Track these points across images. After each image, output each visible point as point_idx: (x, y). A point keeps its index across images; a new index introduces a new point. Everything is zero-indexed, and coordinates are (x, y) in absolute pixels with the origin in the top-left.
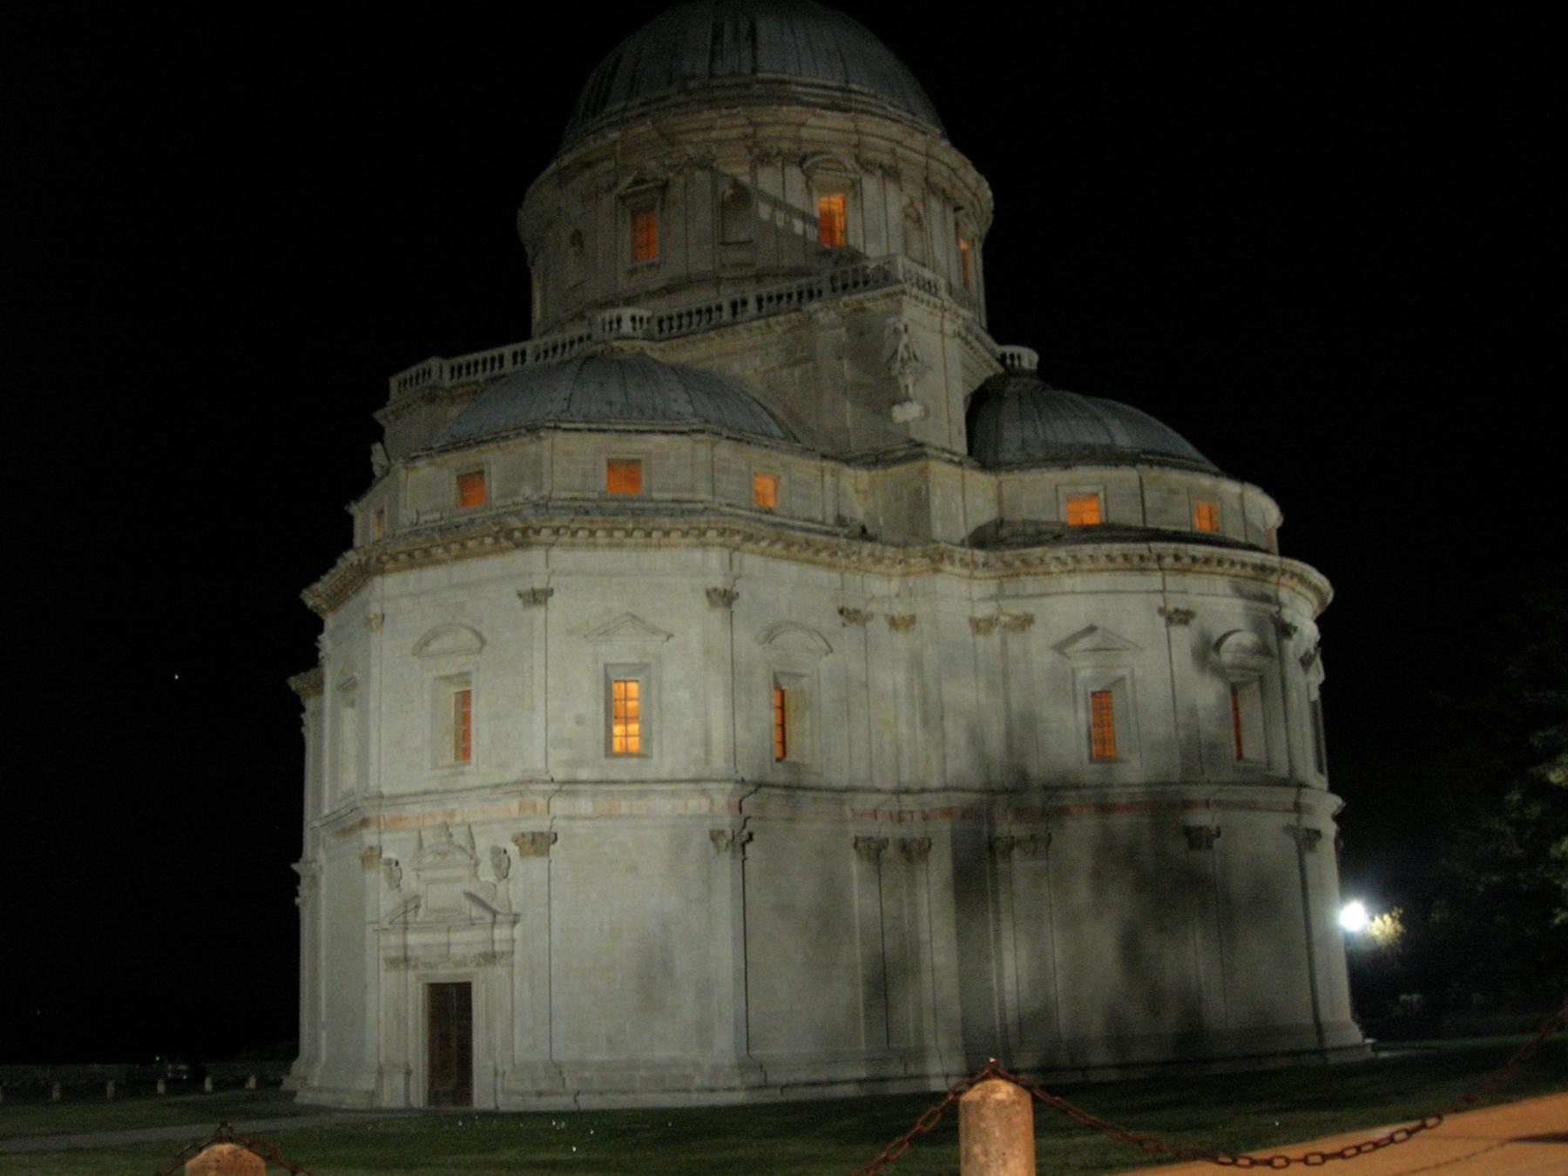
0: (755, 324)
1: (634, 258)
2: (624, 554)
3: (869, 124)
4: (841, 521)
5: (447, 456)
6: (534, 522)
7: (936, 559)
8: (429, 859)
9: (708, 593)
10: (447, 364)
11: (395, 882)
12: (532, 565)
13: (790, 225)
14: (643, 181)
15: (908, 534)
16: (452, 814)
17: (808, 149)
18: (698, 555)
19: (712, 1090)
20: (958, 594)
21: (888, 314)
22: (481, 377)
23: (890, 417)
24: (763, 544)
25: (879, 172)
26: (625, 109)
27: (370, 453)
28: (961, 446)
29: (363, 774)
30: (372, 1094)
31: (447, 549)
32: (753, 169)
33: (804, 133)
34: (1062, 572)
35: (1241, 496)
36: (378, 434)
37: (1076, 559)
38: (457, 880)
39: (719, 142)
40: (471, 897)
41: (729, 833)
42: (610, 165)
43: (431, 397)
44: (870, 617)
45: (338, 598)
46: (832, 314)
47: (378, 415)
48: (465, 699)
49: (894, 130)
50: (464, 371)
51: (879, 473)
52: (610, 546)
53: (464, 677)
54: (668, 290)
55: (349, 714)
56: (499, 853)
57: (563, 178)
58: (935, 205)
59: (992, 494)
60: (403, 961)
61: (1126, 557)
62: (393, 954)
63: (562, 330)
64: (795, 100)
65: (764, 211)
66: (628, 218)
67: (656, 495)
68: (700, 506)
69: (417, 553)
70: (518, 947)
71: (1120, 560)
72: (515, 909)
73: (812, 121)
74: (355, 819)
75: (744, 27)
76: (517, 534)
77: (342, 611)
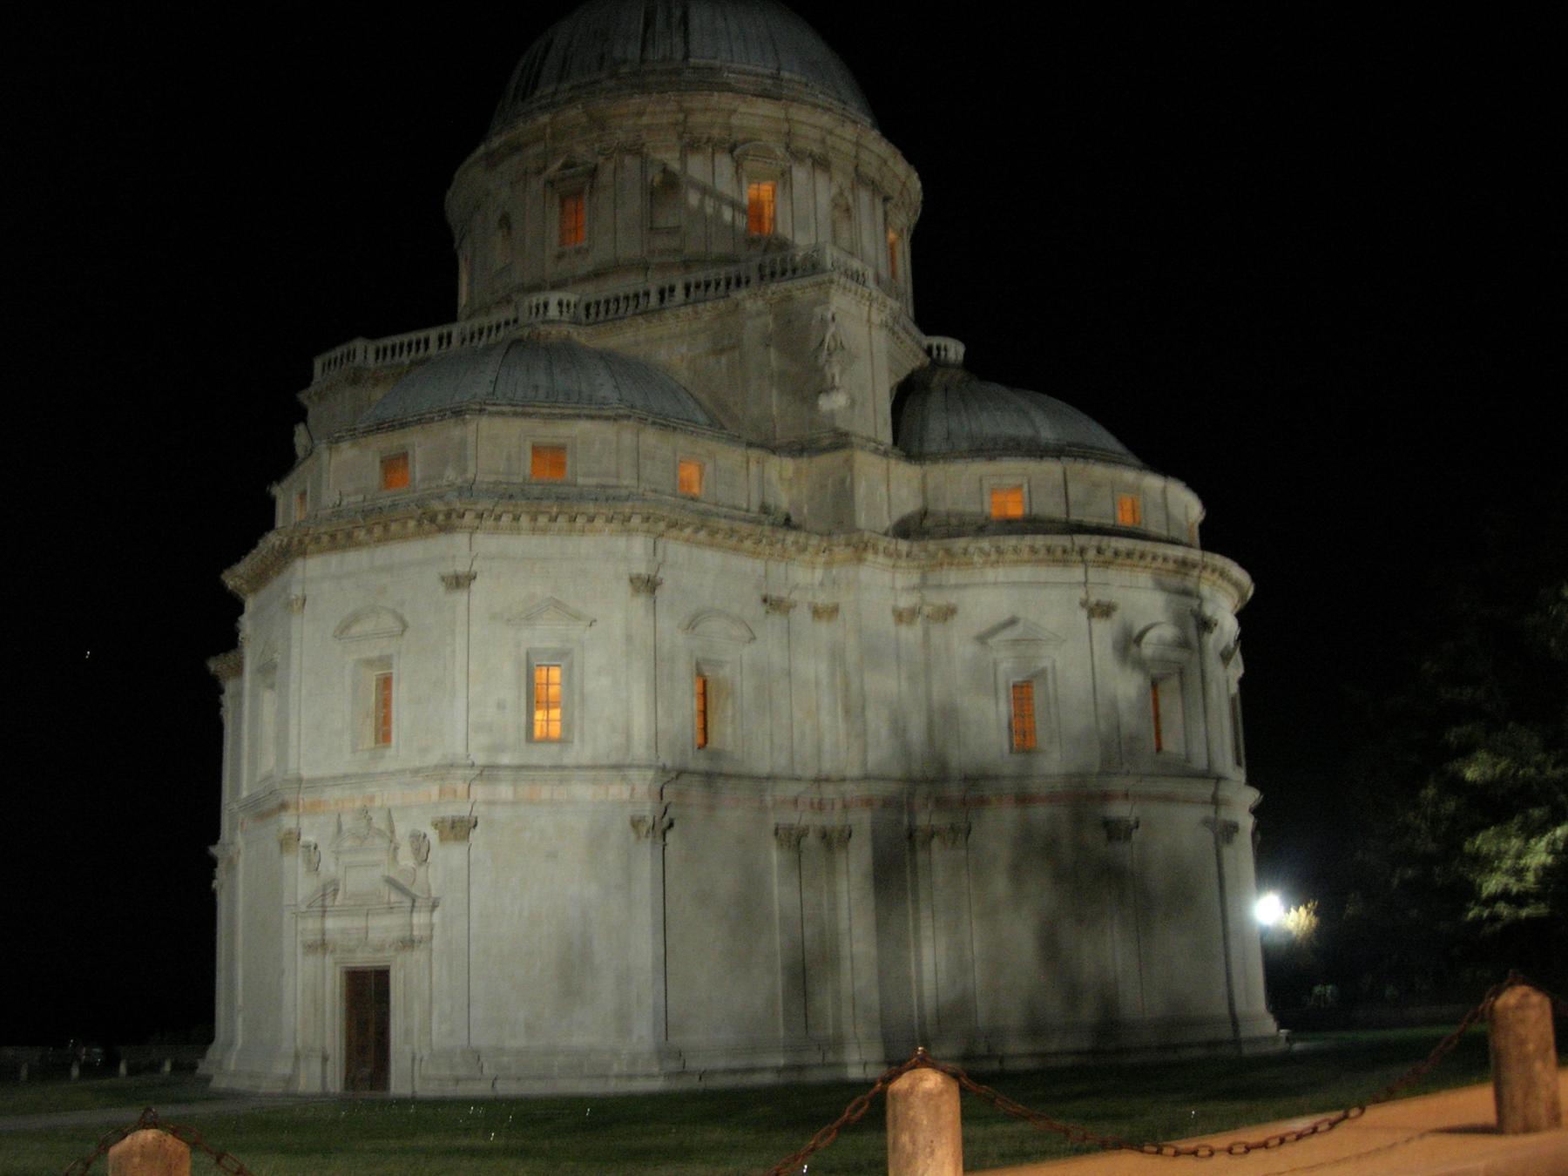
0: (683, 310)
1: (562, 243)
2: (548, 539)
3: (800, 114)
4: (765, 509)
5: (370, 438)
6: (458, 505)
7: (860, 549)
8: (348, 844)
9: (631, 581)
11: (313, 867)
12: (455, 550)
13: (718, 215)
14: (573, 165)
15: (835, 523)
16: (372, 799)
18: (621, 543)
19: (631, 1077)
20: (881, 585)
21: (815, 303)
22: (405, 359)
23: (814, 406)
24: (688, 531)
25: (809, 162)
26: (555, 93)
27: (292, 434)
28: (886, 436)
29: (282, 756)
30: (290, 1080)
31: (370, 531)
32: (683, 160)
33: (735, 121)
34: (986, 562)
35: (1164, 492)
36: (301, 415)
37: (999, 552)
38: (375, 865)
39: (648, 127)
40: (391, 882)
41: (650, 822)
42: (538, 149)
43: (356, 379)
44: (793, 606)
45: (260, 579)
46: (760, 303)
47: (302, 396)
48: (386, 683)
49: (825, 120)
50: (389, 353)
51: (804, 462)
52: (534, 531)
53: (385, 661)
54: (598, 274)
55: (268, 699)
56: (418, 840)
57: (492, 160)
58: (864, 196)
59: (916, 483)
60: (321, 946)
61: (1049, 550)
62: (310, 938)
63: (488, 313)
64: (727, 88)
65: (693, 199)
66: (557, 201)
67: (581, 481)
68: (624, 492)
69: (339, 536)
70: (437, 932)
71: (1043, 551)
72: (434, 894)
73: (743, 108)
74: (273, 803)
75: (677, 13)
76: (441, 517)
77: (263, 594)
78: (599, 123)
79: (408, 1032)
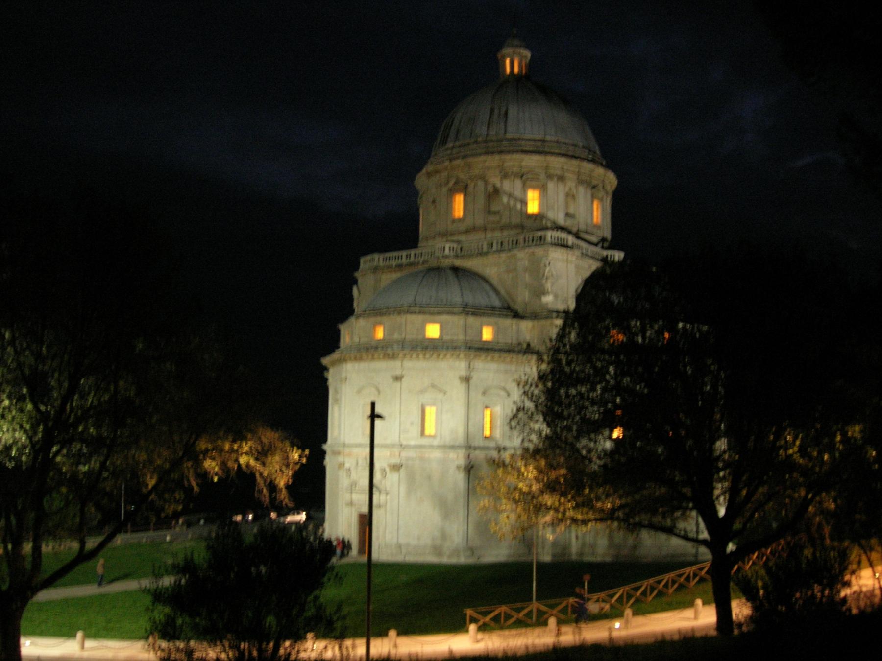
10: (382, 256)
12: (395, 366)
13: (515, 206)
17: (523, 170)
18: (457, 363)
23: (540, 299)
27: (352, 289)
33: (524, 163)
36: (355, 282)
45: (334, 363)
47: (357, 274)
51: (536, 322)
57: (429, 175)
60: (351, 504)
65: (505, 199)
75: (503, 112)
78: (470, 166)
79: (378, 538)
